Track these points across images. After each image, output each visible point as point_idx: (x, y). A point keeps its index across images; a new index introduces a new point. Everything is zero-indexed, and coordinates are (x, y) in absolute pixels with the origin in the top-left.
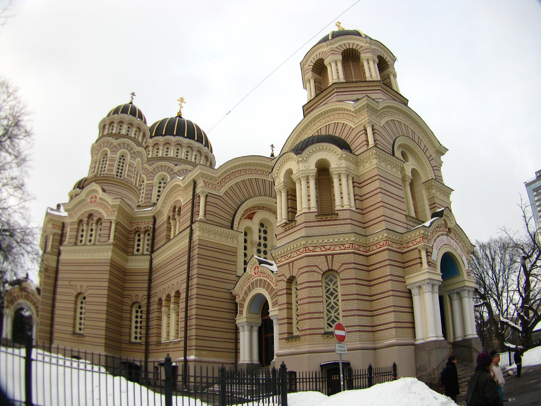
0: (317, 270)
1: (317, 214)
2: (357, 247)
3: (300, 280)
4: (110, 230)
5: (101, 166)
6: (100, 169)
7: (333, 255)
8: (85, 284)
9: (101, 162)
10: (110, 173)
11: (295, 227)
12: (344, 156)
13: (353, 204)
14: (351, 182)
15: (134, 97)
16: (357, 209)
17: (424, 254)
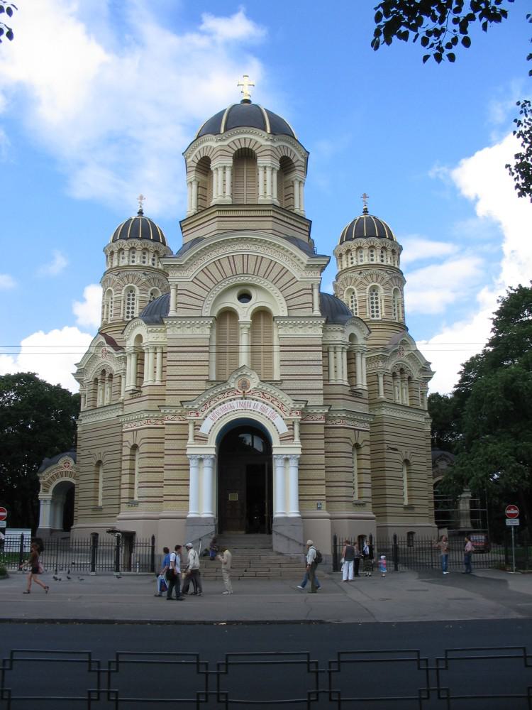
0: (128, 445)
1: (131, 392)
2: (153, 421)
3: (142, 449)
4: (121, 385)
5: (110, 309)
6: (110, 313)
7: (136, 430)
8: (102, 450)
9: (110, 305)
10: (117, 317)
11: (141, 397)
12: (150, 329)
13: (158, 377)
14: (159, 355)
15: (143, 201)
16: (162, 381)
17: (191, 427)
